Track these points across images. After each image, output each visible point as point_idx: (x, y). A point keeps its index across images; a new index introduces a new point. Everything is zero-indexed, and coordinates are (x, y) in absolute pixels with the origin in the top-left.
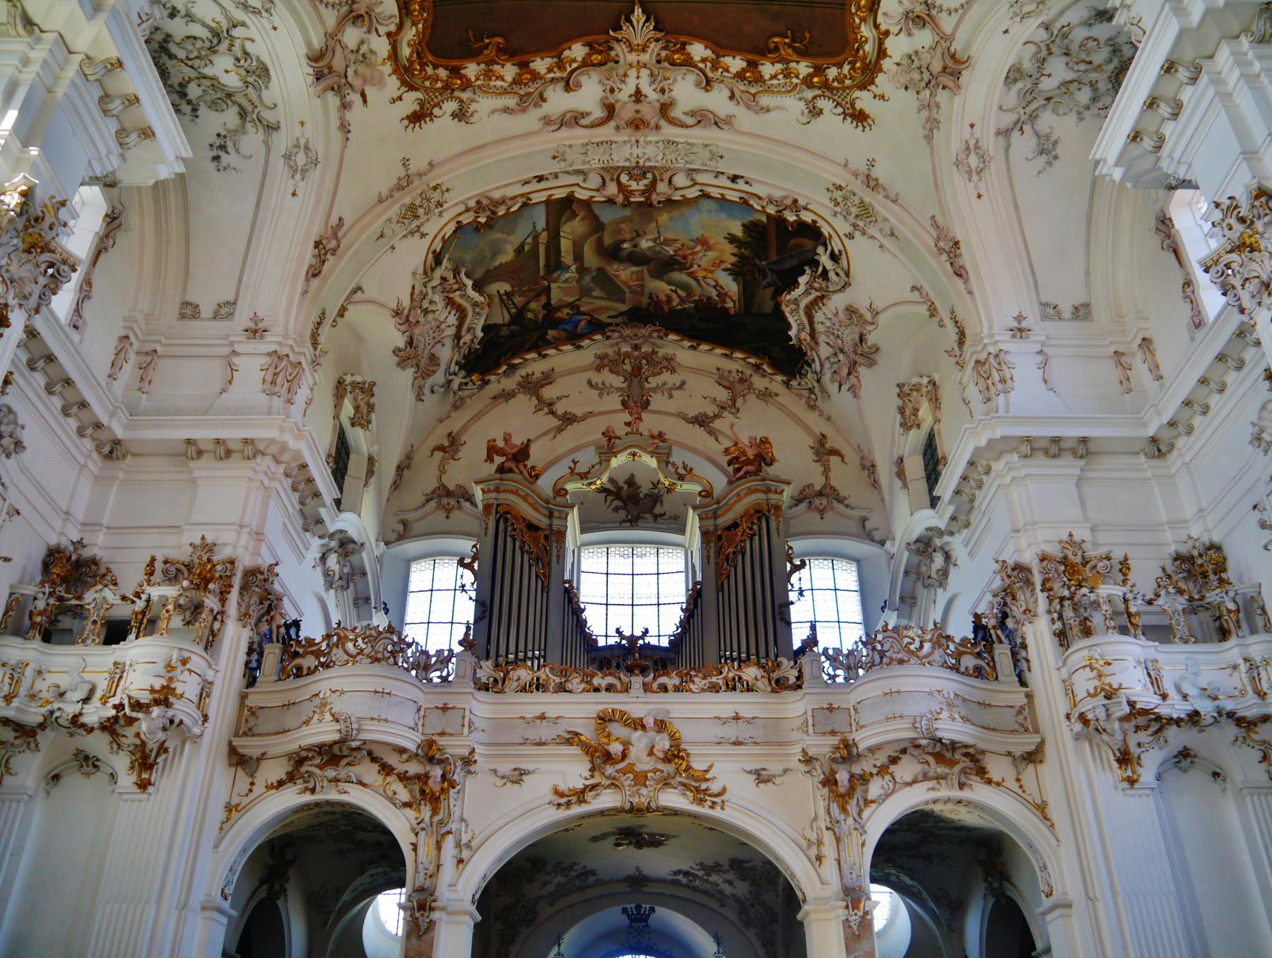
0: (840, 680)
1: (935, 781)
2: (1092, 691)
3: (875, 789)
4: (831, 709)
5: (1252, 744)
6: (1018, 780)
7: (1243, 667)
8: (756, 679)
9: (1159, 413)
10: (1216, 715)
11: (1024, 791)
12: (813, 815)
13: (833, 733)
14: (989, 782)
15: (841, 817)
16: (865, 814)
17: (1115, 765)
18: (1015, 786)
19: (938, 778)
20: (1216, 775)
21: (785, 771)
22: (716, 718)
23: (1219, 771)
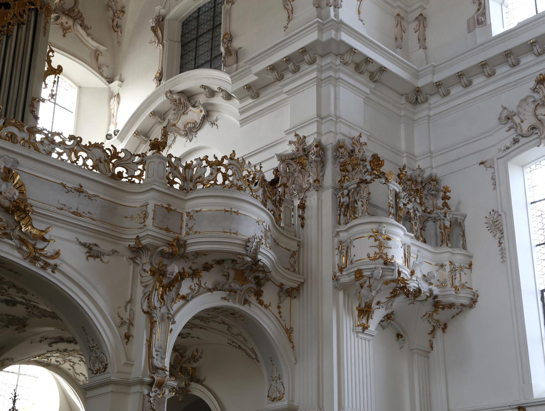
0: (177, 186)
1: (228, 293)
2: (372, 255)
3: (185, 288)
4: (169, 209)
5: (431, 321)
6: (279, 307)
7: (448, 268)
8: (100, 162)
9: (433, 73)
10: (428, 295)
11: (281, 317)
12: (129, 298)
13: (167, 230)
14: (261, 303)
15: (157, 304)
16: (175, 307)
17: (356, 313)
18: (276, 312)
19: (231, 291)
20: (399, 336)
21: (114, 252)
22: (62, 184)
23: (402, 333)
